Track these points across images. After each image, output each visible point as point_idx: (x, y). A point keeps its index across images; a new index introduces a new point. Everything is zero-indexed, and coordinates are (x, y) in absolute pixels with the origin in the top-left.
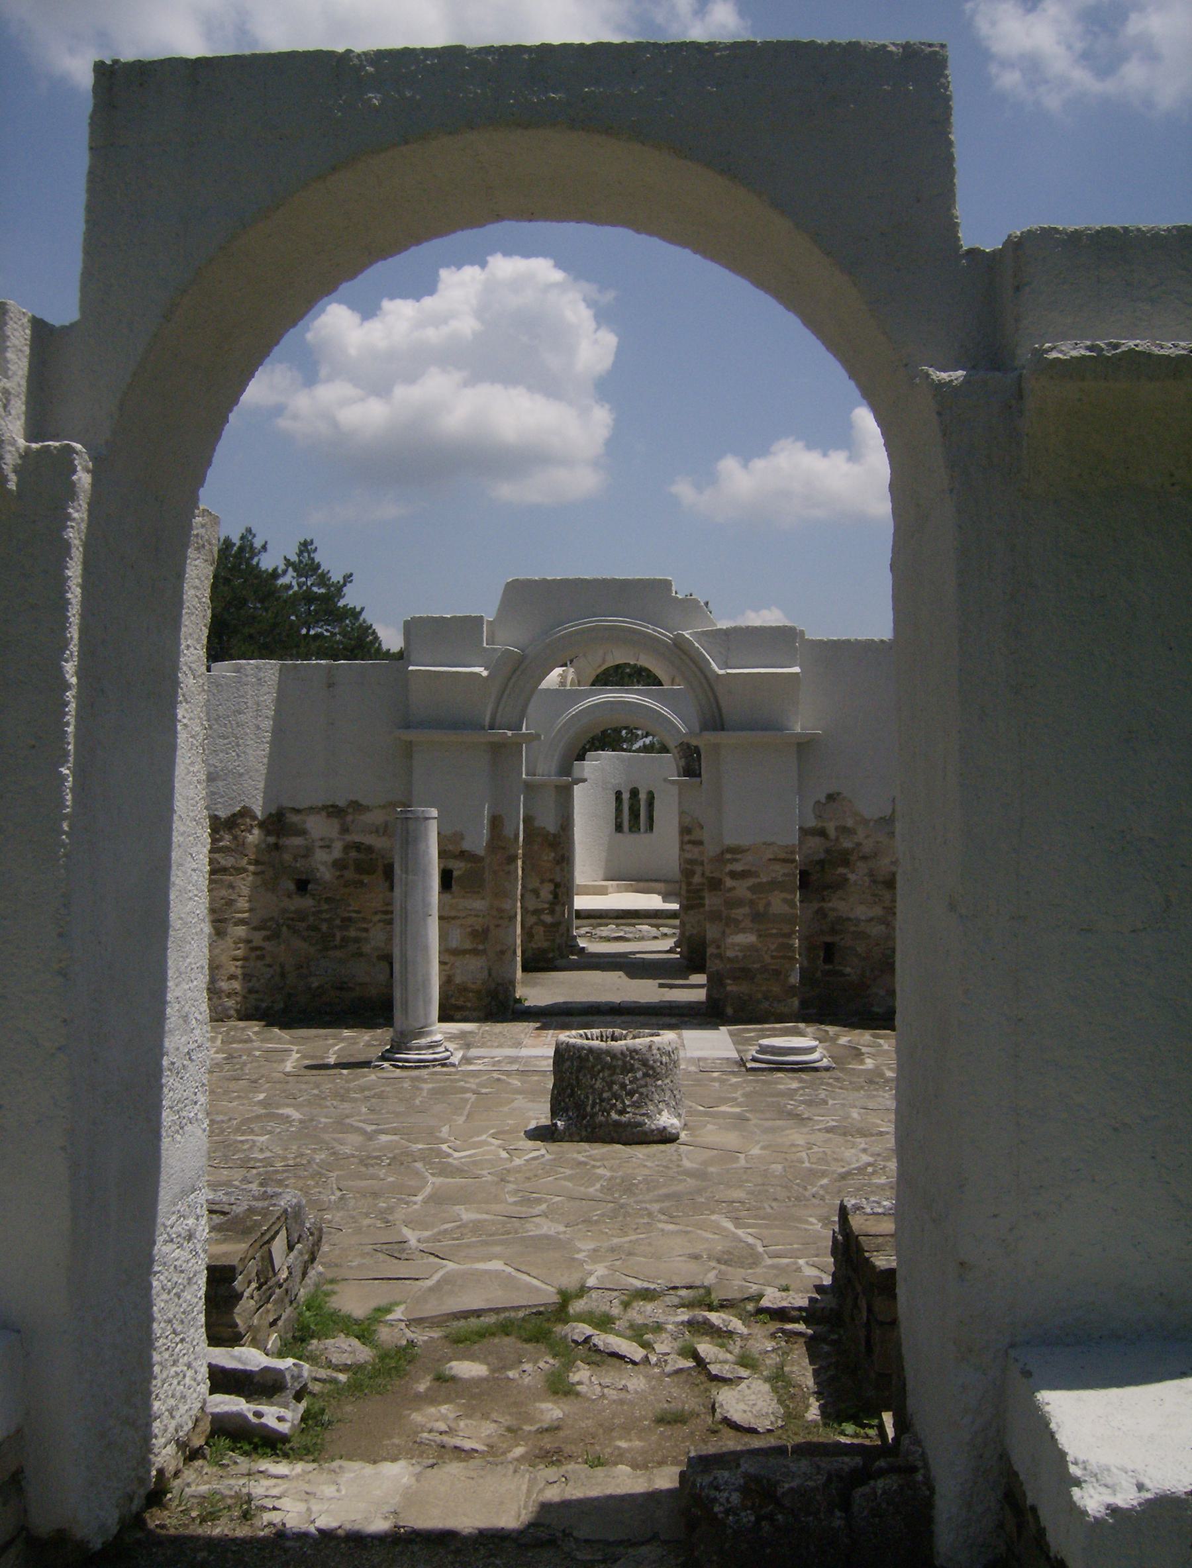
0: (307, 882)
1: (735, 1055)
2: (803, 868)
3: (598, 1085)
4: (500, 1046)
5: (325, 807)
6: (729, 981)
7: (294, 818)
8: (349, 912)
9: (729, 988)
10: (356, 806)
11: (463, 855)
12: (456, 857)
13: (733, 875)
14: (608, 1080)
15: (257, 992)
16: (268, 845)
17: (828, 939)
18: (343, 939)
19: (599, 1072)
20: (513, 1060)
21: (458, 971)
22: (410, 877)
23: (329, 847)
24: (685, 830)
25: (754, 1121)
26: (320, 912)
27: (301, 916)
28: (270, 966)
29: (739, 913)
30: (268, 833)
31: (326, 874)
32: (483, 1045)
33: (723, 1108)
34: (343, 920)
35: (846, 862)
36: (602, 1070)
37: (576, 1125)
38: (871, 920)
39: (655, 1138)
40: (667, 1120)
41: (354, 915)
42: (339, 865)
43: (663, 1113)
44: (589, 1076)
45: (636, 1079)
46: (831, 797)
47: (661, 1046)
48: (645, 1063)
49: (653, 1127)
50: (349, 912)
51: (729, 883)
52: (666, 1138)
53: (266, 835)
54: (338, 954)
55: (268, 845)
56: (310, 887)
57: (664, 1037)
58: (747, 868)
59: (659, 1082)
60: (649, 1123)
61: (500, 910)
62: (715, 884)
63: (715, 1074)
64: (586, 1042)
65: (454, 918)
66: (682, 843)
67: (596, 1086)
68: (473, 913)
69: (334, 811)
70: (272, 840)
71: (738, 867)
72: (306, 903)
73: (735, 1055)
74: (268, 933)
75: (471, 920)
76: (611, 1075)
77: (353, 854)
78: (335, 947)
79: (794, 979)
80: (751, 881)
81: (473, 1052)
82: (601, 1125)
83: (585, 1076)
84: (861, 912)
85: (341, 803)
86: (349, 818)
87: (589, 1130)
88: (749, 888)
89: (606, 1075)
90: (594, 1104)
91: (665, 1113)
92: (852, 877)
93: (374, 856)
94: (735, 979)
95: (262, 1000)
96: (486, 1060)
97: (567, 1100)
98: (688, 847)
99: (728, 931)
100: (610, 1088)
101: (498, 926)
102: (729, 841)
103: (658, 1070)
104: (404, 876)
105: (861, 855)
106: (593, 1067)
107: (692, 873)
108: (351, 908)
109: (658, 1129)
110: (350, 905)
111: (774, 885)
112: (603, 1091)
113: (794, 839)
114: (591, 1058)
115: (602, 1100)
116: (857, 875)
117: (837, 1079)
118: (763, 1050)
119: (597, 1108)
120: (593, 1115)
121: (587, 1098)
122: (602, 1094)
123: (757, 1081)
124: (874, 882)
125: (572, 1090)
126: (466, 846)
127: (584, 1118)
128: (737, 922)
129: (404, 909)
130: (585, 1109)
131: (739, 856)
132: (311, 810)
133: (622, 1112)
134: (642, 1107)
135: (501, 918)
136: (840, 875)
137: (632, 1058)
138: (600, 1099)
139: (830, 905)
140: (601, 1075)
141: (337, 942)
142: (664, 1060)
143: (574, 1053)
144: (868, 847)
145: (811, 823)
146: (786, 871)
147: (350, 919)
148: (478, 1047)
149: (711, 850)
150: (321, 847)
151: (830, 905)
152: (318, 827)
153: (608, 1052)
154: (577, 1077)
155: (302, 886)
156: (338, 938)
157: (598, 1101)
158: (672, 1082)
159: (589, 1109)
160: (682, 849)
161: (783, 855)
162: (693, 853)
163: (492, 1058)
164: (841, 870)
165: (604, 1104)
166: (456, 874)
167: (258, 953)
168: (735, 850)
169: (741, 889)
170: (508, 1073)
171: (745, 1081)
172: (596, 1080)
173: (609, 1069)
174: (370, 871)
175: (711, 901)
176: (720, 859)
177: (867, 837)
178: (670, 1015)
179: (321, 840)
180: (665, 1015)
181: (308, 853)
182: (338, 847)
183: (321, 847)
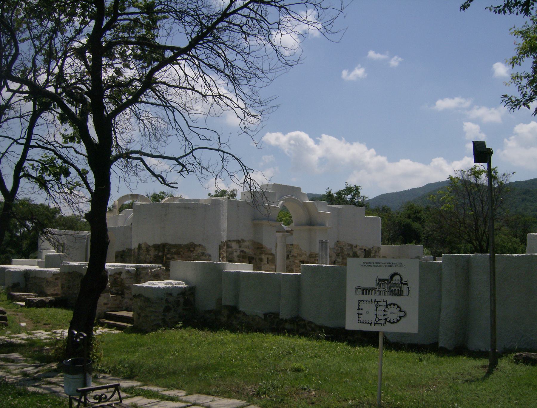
5: (236, 240)
7: (229, 243)
10: (243, 240)
69: (238, 242)
77: (242, 254)
85: (240, 240)
86: (241, 243)
132: (233, 241)
152: (234, 246)
182: (239, 251)
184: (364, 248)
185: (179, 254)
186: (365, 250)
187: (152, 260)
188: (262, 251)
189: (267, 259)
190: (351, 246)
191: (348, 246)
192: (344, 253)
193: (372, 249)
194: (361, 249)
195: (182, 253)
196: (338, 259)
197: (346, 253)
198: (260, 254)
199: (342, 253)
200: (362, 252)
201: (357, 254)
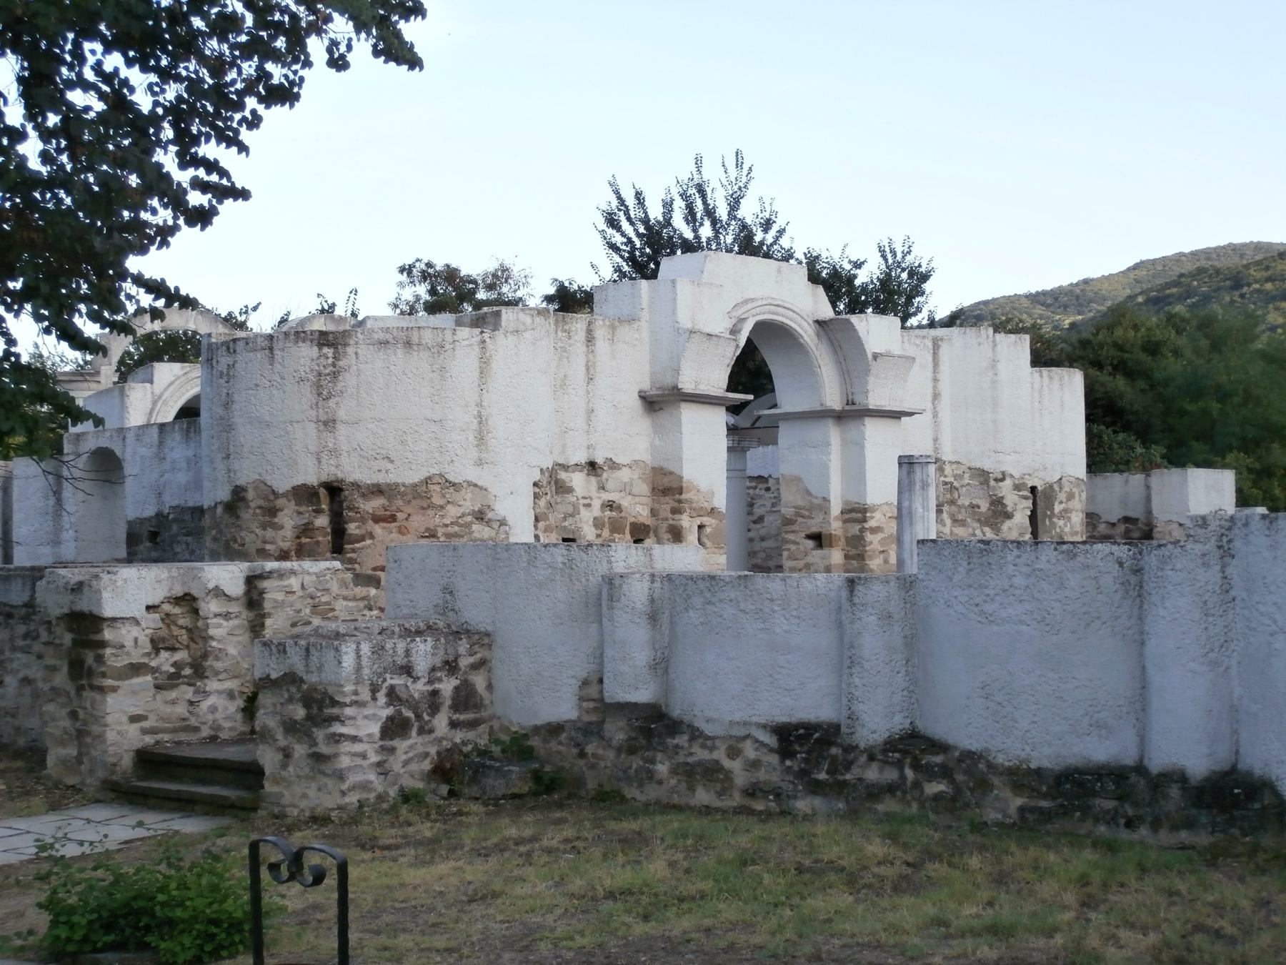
7: (563, 475)
10: (614, 466)
77: (608, 513)
85: (600, 461)
86: (605, 475)
93: (623, 514)
150: (584, 505)
174: (621, 531)
179: (584, 498)
182: (597, 504)
183: (584, 505)
185: (393, 518)
186: (1033, 489)
187: (285, 545)
188: (680, 501)
189: (701, 527)
190: (982, 476)
191: (971, 477)
192: (960, 503)
193: (1056, 487)
194: (1017, 487)
195: (400, 516)
197: (967, 503)
198: (676, 511)
199: (952, 502)
201: (1004, 506)
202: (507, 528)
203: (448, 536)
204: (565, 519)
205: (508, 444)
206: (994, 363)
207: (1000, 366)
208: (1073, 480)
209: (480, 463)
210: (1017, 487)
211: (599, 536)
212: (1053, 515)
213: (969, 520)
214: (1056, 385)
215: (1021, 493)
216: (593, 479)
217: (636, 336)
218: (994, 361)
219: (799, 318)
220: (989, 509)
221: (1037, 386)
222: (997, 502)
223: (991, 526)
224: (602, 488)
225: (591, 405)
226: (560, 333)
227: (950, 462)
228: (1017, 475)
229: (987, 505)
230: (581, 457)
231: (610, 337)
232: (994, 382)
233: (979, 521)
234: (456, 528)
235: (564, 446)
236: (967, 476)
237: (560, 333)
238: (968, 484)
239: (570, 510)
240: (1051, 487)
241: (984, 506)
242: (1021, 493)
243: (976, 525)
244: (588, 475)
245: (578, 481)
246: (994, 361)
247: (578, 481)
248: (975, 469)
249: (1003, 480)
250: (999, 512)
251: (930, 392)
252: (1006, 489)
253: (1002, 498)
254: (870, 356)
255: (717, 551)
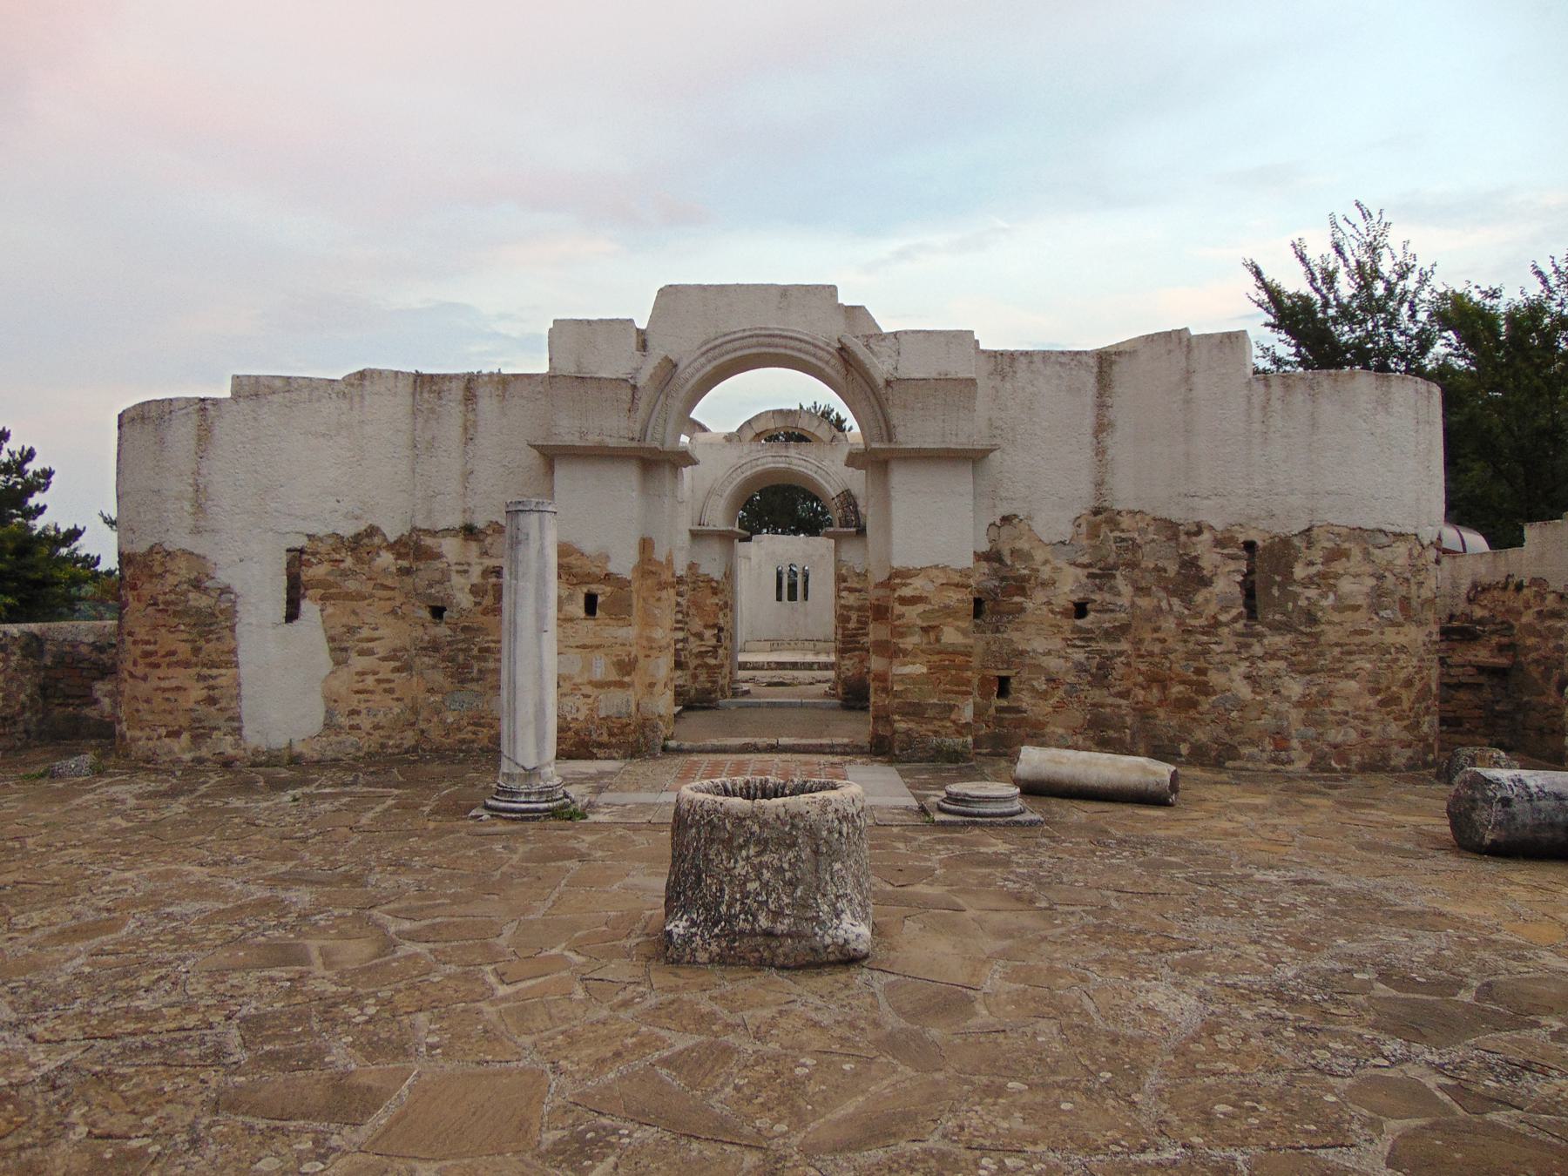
0: (444, 609)
1: (914, 803)
2: (977, 596)
3: (741, 868)
4: (638, 789)
6: (897, 717)
7: (428, 541)
8: (487, 642)
9: (897, 725)
11: (608, 578)
12: (599, 581)
13: (904, 601)
14: (756, 861)
15: (382, 728)
16: (399, 570)
17: (1003, 673)
18: (480, 671)
19: (741, 847)
20: (646, 807)
21: (602, 705)
22: (521, 584)
23: (466, 572)
24: (840, 578)
25: (970, 913)
26: (458, 642)
27: (434, 647)
28: (398, 700)
29: (910, 642)
30: (399, 556)
31: (465, 600)
32: (619, 789)
33: (921, 888)
34: (481, 650)
35: (1022, 591)
36: (745, 845)
37: (702, 936)
38: (1049, 653)
39: (832, 957)
40: (854, 930)
41: (493, 645)
42: (475, 590)
43: (843, 916)
44: (724, 855)
45: (799, 858)
46: (1006, 519)
47: (840, 807)
48: (812, 832)
49: (828, 940)
50: (487, 642)
51: (898, 609)
52: (849, 959)
53: (396, 559)
54: (475, 687)
55: (399, 570)
56: (446, 614)
57: (844, 791)
58: (917, 593)
59: (837, 866)
60: (820, 933)
61: (650, 639)
62: (880, 612)
63: (895, 830)
64: (720, 799)
65: (598, 647)
66: (839, 590)
67: (736, 872)
68: (619, 641)
70: (404, 563)
71: (906, 592)
72: (442, 631)
73: (914, 803)
74: (398, 664)
75: (618, 649)
76: (759, 854)
78: (472, 680)
79: (967, 714)
80: (920, 608)
81: (606, 797)
82: (742, 932)
83: (718, 853)
84: (1039, 644)
86: (489, 540)
87: (724, 944)
88: (918, 615)
89: (752, 852)
90: (733, 901)
91: (847, 918)
92: (1029, 605)
94: (904, 715)
95: (389, 737)
96: (614, 809)
97: (690, 893)
98: (844, 594)
99: (895, 661)
100: (759, 877)
101: (647, 656)
102: (897, 563)
103: (835, 846)
104: (514, 582)
105: (1039, 580)
106: (731, 839)
107: (848, 619)
108: (490, 638)
109: (834, 943)
110: (488, 635)
111: (948, 612)
112: (746, 880)
113: (968, 562)
114: (729, 826)
115: (746, 895)
116: (1034, 603)
117: (1052, 839)
118: (953, 798)
119: (738, 906)
120: (731, 919)
121: (722, 890)
122: (745, 883)
123: (952, 841)
124: (1052, 612)
125: (699, 877)
126: (612, 568)
127: (715, 924)
128: (905, 653)
129: (514, 623)
130: (717, 910)
131: (909, 581)
132: (447, 531)
133: (777, 915)
134: (810, 907)
135: (651, 648)
136: (1017, 603)
137: (793, 826)
138: (741, 892)
139: (1005, 636)
140: (744, 853)
141: (475, 674)
142: (845, 830)
143: (702, 817)
144: (1045, 573)
145: (985, 547)
146: (959, 596)
147: (488, 650)
148: (611, 791)
149: (879, 576)
150: (458, 572)
151: (1005, 636)
153: (754, 816)
154: (706, 855)
155: (438, 612)
156: (475, 671)
157: (738, 896)
158: (856, 862)
159: (723, 909)
160: (838, 597)
161: (957, 579)
162: (851, 599)
163: (624, 805)
164: (1017, 599)
165: (748, 901)
166: (600, 599)
167: (387, 686)
168: (905, 574)
169: (912, 613)
170: (635, 828)
171: (940, 841)
172: (736, 862)
173: (758, 842)
175: (875, 632)
176: (887, 584)
177: (1046, 562)
178: (832, 753)
180: (824, 753)
181: (444, 578)
183: (458, 572)
184: (1242, 538)
186: (1250, 546)
190: (1170, 528)
196: (1097, 597)
197: (1152, 566)
199: (1133, 565)
200: (1233, 558)
201: (1199, 568)
202: (232, 597)
203: (167, 603)
204: (430, 586)
205: (238, 511)
206: (1188, 374)
207: (1195, 379)
208: (1345, 531)
209: (197, 531)
210: (1219, 543)
211: (477, 604)
212: (1288, 577)
213: (1154, 588)
214: (1299, 397)
215: (1225, 551)
216: (474, 547)
217: (540, 389)
218: (1188, 372)
219: (811, 348)
220: (1179, 573)
221: (1257, 400)
222: (1190, 565)
223: (1180, 596)
224: (485, 553)
225: (469, 466)
226: (426, 395)
227: (1130, 512)
228: (1219, 526)
229: (1176, 567)
230: (456, 521)
231: (500, 393)
232: (1187, 401)
233: (1165, 589)
234: (173, 597)
235: (430, 512)
236: (1151, 529)
237: (426, 395)
238: (1153, 540)
239: (438, 576)
240: (1286, 542)
241: (1172, 569)
242: (1225, 551)
243: (1162, 594)
244: (466, 539)
245: (451, 548)
246: (1188, 372)
247: (451, 548)
248: (1161, 519)
249: (1199, 532)
250: (1192, 577)
251: (1089, 422)
252: (1203, 548)
253: (1196, 558)
254: (881, 383)
255: (611, 622)
